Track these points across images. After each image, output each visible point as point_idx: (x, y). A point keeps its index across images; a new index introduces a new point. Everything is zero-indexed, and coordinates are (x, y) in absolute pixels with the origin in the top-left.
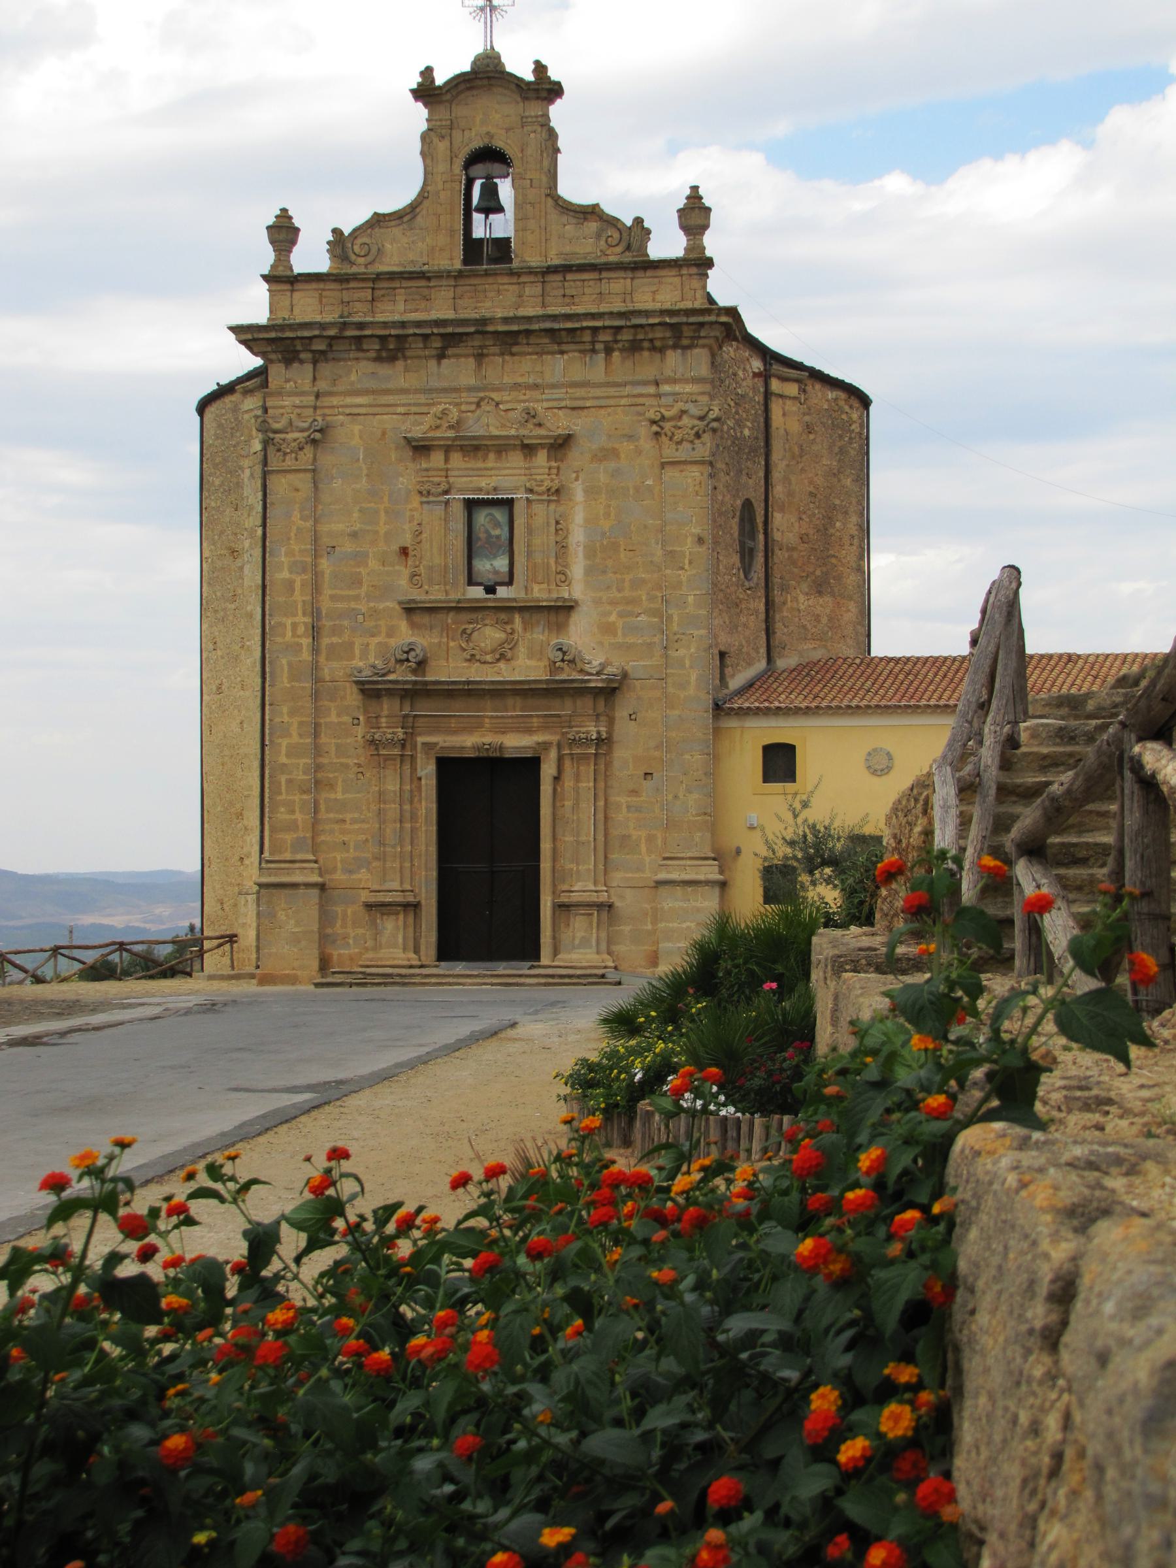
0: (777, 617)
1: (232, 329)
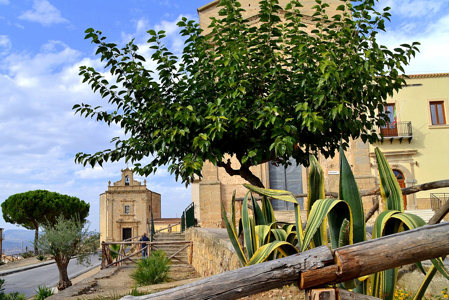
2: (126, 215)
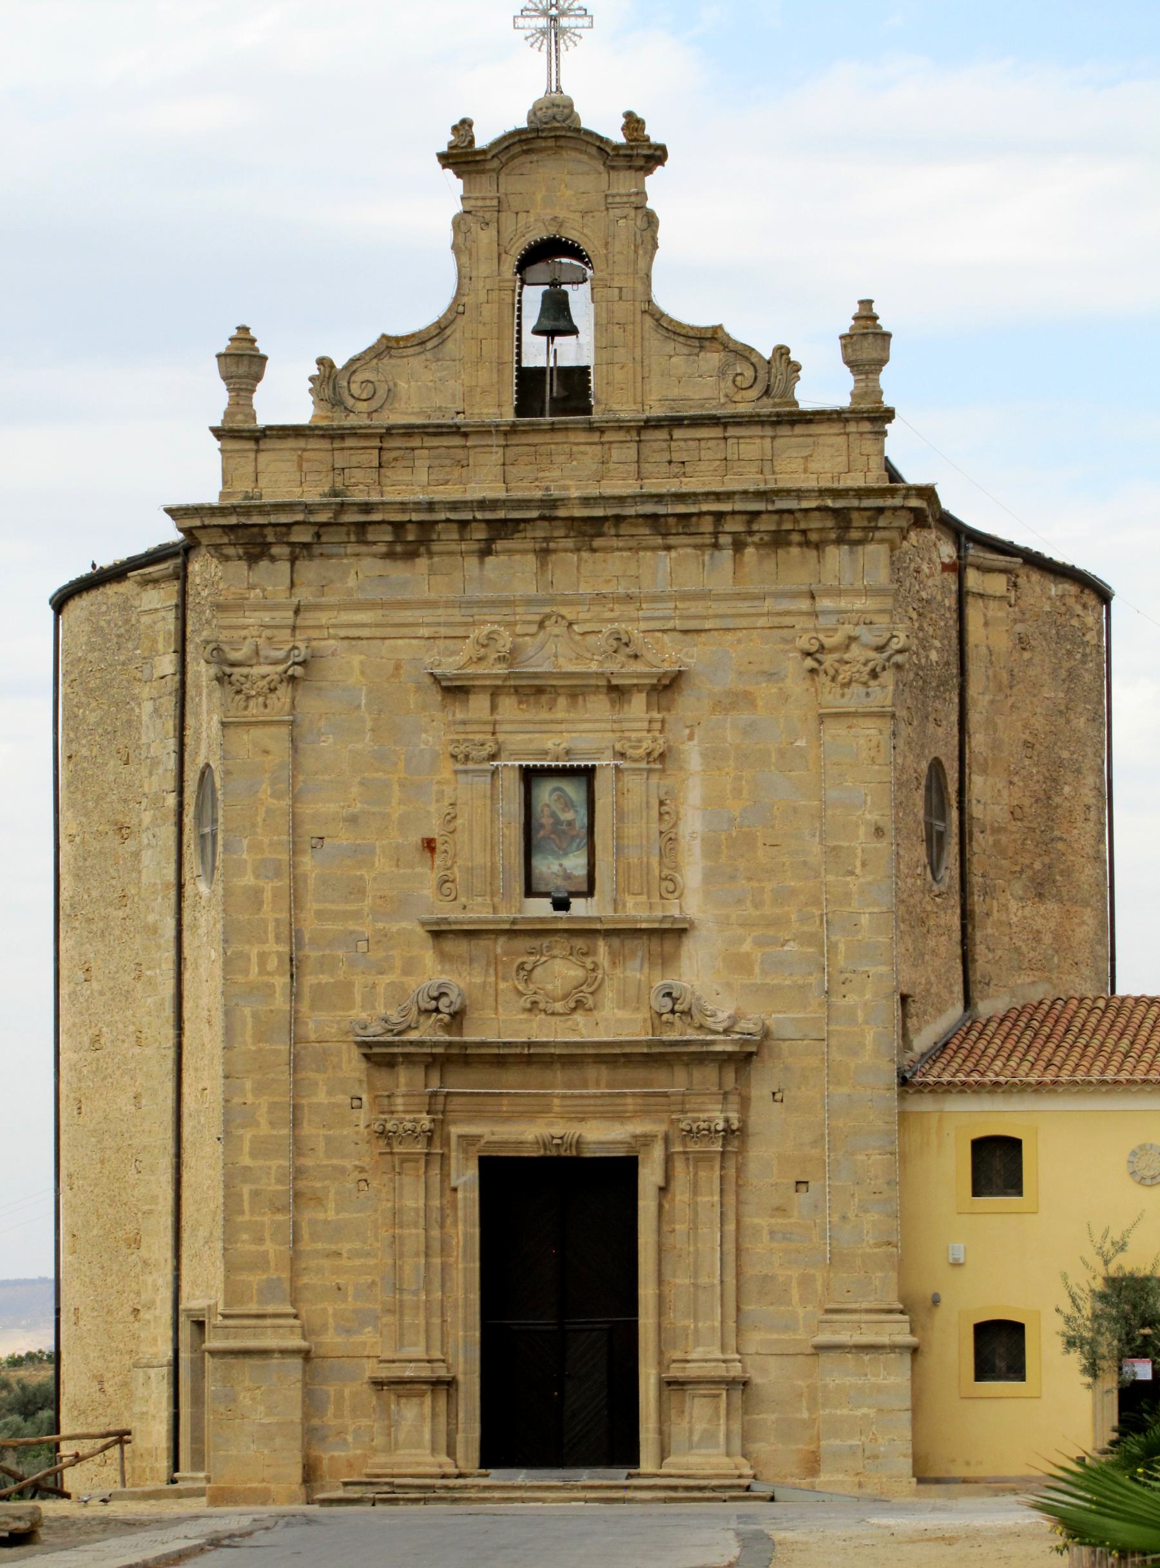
0: (979, 936)
1: (170, 511)
2: (539, 932)
